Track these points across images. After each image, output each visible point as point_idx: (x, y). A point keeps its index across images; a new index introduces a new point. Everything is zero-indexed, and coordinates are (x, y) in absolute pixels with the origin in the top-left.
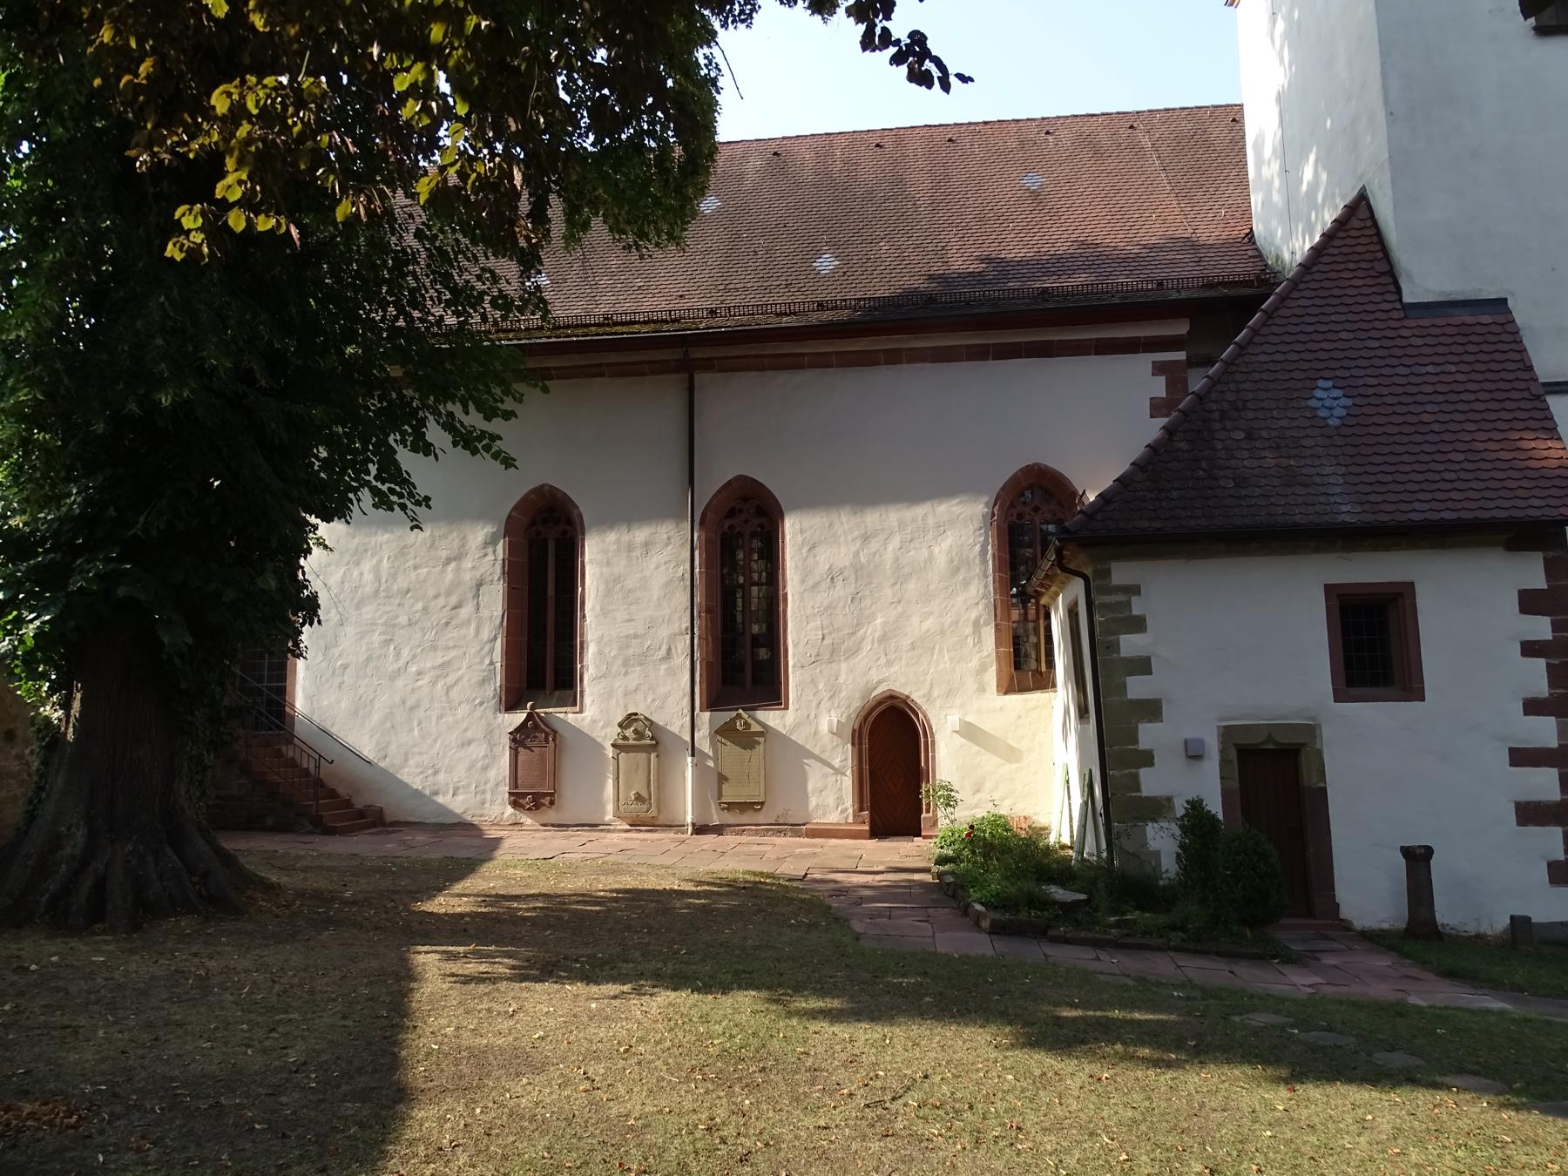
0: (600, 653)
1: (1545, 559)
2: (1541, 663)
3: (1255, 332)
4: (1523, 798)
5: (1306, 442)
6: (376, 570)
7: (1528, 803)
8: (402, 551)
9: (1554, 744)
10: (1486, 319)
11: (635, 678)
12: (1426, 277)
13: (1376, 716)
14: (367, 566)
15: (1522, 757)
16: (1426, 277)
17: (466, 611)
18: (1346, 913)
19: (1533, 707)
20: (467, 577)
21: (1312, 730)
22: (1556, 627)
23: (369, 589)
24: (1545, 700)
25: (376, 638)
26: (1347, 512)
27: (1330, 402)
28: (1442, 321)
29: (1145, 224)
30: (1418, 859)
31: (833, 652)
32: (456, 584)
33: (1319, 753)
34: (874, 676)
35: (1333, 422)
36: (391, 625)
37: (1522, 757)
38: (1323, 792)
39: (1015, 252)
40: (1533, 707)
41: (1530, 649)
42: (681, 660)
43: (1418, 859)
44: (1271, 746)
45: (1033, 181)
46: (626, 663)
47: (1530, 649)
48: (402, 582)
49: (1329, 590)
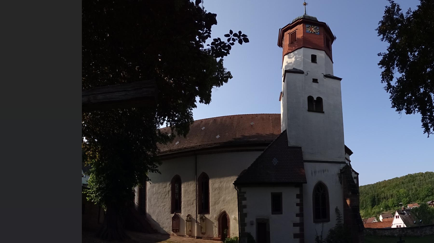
0: (184, 203)
6: (156, 189)
8: (159, 186)
11: (189, 208)
14: (154, 189)
17: (167, 196)
20: (167, 190)
23: (155, 192)
25: (156, 200)
29: (268, 131)
31: (215, 203)
32: (166, 191)
34: (222, 208)
36: (158, 198)
41: (297, 205)
42: (195, 205)
46: (188, 205)
48: (159, 191)
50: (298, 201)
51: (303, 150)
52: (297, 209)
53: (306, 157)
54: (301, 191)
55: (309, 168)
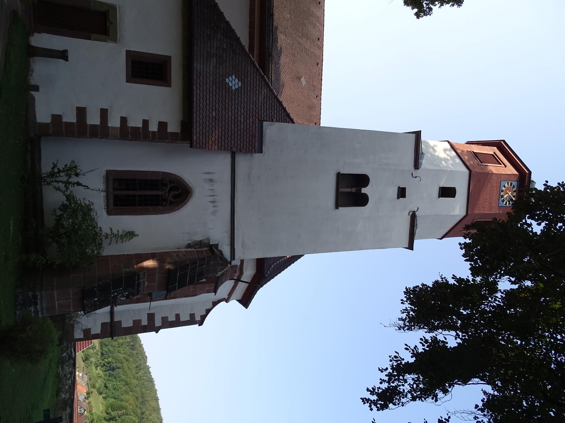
1: (178, 133)
2: (140, 125)
3: (258, 70)
4: (88, 111)
5: (221, 66)
7: (86, 112)
9: (109, 125)
10: (257, 143)
12: (272, 130)
13: (121, 65)
15: (104, 113)
16: (272, 130)
18: (36, 35)
19: (124, 120)
21: (115, 40)
22: (153, 133)
24: (126, 124)
26: (197, 66)
27: (234, 83)
28: (257, 129)
30: (63, 55)
33: (106, 41)
35: (227, 80)
37: (104, 113)
38: (90, 39)
39: (284, 60)
40: (124, 120)
41: (146, 123)
43: (63, 55)
44: (108, 24)
45: (303, 80)
47: (146, 123)
49: (169, 57)
50: (153, 128)
51: (256, 155)
52: (135, 122)
53: (242, 161)
54: (174, 138)
55: (220, 164)
